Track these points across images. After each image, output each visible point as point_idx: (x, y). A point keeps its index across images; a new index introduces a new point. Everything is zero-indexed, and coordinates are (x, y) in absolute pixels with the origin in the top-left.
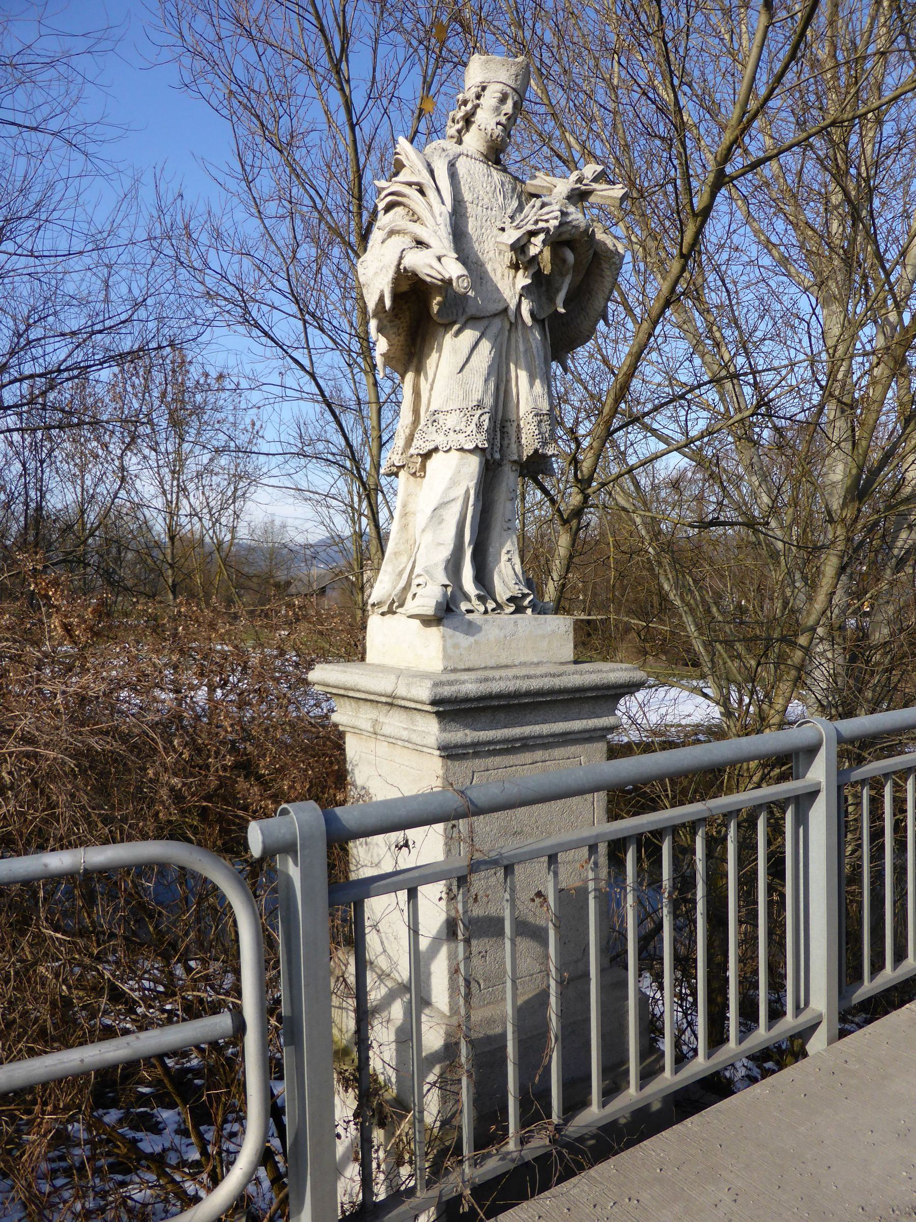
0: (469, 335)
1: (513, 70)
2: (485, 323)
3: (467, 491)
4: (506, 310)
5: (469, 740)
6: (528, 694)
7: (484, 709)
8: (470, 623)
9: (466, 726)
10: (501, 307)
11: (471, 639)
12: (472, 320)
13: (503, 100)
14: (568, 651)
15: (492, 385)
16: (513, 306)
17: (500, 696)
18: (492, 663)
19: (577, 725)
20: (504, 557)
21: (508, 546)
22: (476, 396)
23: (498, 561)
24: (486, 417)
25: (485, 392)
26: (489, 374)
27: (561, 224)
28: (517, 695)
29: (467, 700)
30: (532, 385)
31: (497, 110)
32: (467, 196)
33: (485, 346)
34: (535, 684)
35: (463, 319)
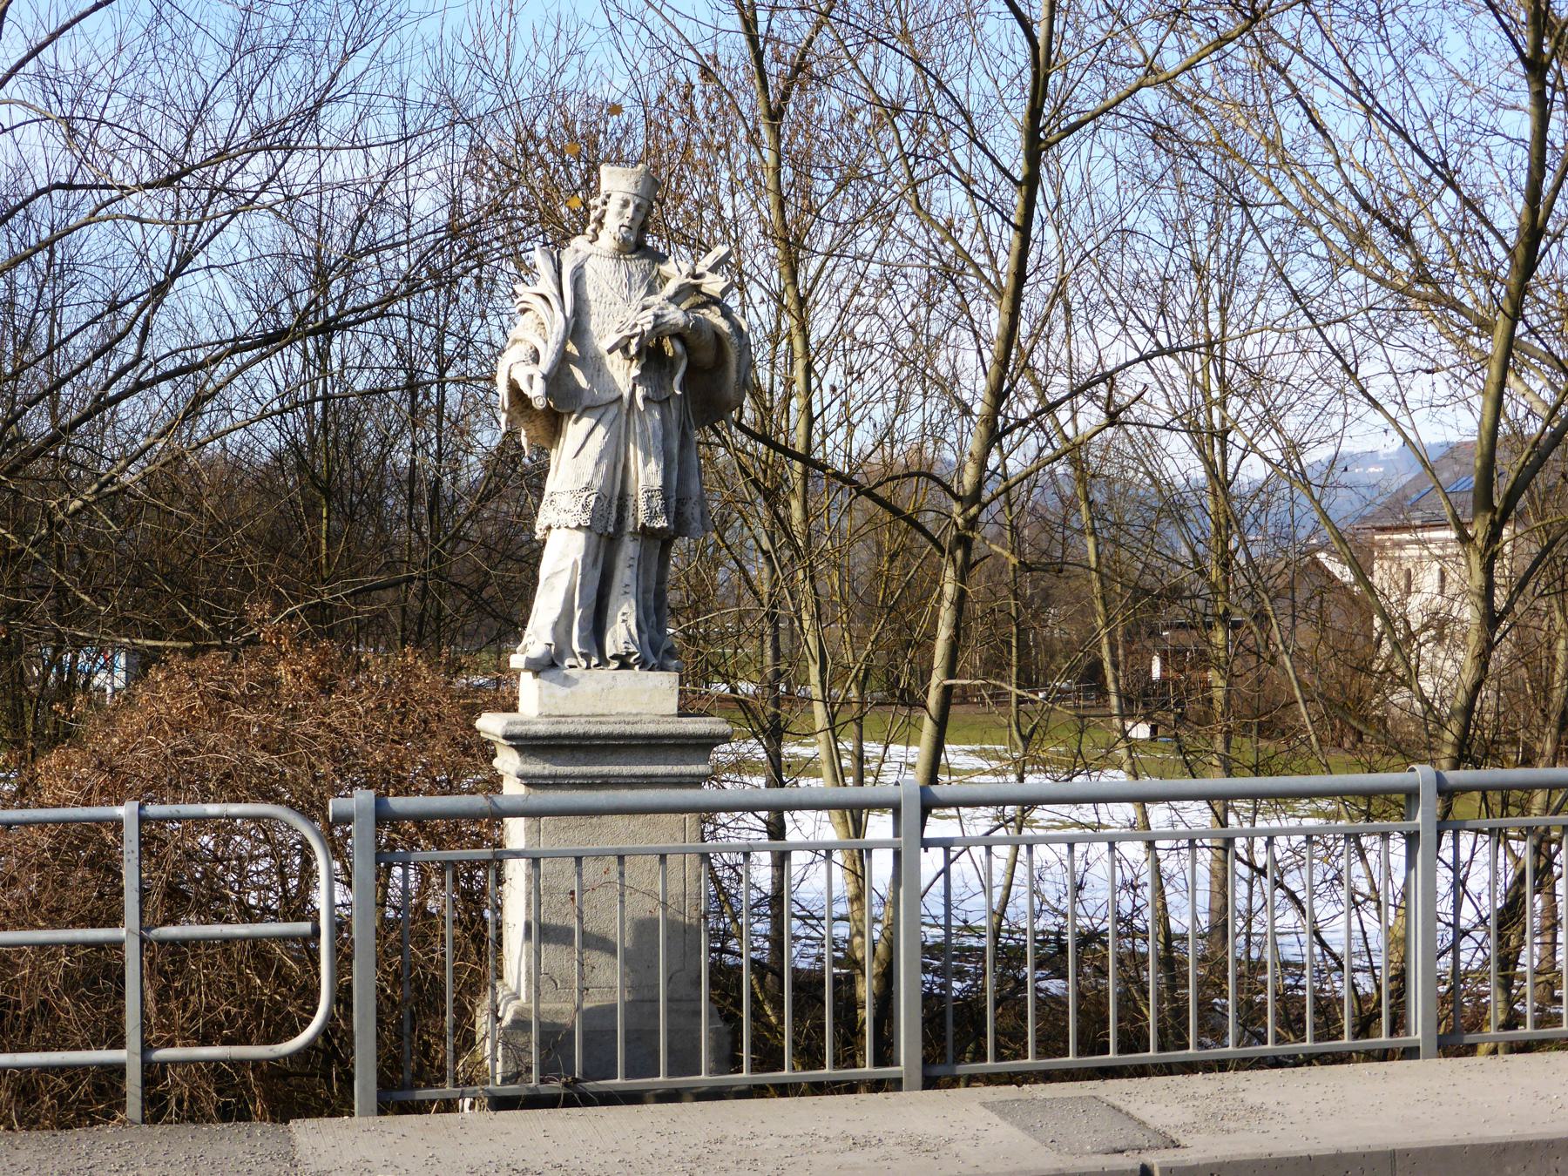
0: (587, 423)
1: (633, 179)
2: (598, 413)
3: (575, 562)
4: (621, 397)
5: (546, 772)
6: (598, 736)
7: (562, 747)
8: (566, 677)
9: (546, 761)
10: (616, 395)
11: (567, 690)
12: (586, 410)
13: (625, 204)
14: (672, 705)
15: (603, 468)
16: (626, 395)
17: (569, 736)
18: (588, 712)
20: (620, 618)
21: (625, 608)
22: (587, 479)
23: (614, 622)
24: (593, 498)
25: (595, 474)
26: (601, 458)
27: (654, 328)
28: (586, 736)
29: (536, 737)
30: (645, 465)
31: (620, 215)
32: (591, 294)
33: (601, 430)
34: (604, 729)
35: (579, 410)
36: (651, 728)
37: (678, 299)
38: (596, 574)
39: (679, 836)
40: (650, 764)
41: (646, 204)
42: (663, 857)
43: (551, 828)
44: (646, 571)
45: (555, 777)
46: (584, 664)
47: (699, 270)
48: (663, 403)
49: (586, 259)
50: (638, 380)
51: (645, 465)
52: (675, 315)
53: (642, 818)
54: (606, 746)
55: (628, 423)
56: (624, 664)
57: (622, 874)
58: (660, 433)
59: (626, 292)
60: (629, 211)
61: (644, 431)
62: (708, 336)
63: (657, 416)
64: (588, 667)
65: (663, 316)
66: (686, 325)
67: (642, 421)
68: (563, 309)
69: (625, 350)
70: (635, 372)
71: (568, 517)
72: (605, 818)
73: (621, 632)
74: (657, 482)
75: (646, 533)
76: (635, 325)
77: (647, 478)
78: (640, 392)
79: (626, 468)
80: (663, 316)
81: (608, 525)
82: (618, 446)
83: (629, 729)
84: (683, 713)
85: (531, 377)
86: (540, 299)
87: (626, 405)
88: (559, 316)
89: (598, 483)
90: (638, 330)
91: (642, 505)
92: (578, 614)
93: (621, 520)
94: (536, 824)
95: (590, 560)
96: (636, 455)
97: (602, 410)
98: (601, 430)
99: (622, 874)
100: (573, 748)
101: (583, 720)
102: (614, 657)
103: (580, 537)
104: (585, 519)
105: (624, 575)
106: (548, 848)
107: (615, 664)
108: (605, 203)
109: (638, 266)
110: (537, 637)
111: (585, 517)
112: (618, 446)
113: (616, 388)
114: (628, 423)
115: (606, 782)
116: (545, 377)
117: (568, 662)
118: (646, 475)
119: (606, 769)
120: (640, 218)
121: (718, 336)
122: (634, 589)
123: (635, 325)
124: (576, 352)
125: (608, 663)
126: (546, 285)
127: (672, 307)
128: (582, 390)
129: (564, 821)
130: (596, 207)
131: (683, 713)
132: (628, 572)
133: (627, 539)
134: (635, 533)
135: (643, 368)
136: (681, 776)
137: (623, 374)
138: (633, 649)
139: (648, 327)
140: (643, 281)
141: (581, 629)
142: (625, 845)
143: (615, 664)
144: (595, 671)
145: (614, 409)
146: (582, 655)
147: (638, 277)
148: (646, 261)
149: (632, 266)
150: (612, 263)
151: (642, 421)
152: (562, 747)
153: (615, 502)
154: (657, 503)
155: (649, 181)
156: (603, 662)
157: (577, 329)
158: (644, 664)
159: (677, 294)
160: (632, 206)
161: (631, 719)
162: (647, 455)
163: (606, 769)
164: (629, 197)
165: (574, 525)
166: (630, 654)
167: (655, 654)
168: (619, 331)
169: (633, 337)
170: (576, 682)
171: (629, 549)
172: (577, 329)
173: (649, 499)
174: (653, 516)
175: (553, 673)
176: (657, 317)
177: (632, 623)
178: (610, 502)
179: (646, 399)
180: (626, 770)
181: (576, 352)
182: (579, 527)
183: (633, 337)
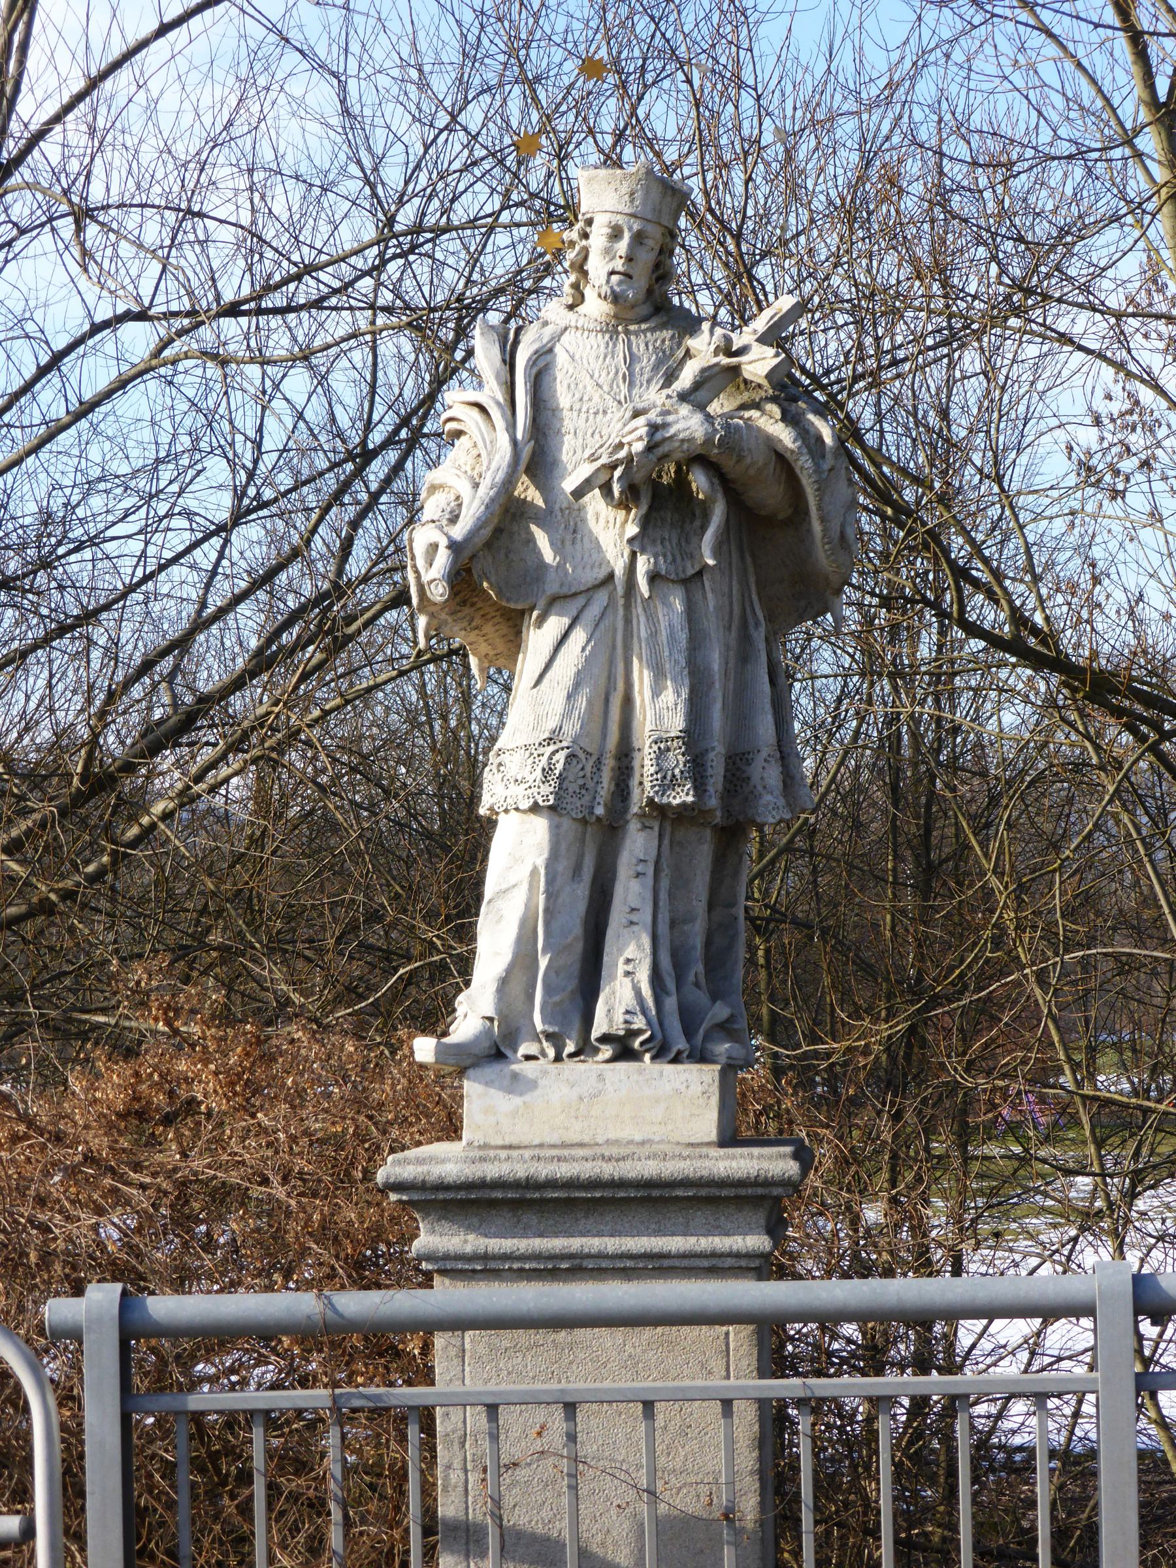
0: (555, 624)
1: (625, 189)
2: (574, 606)
3: (534, 872)
4: (611, 576)
5: (468, 1249)
6: (552, 1184)
7: (493, 1204)
8: (515, 1076)
9: (470, 1228)
10: (602, 574)
11: (517, 1101)
12: (555, 602)
13: (616, 234)
14: (707, 1125)
15: (582, 703)
16: (619, 569)
17: (499, 1184)
18: (554, 1139)
19: (704, 1243)
20: (621, 968)
21: (630, 951)
22: (552, 724)
23: (613, 977)
24: (561, 757)
25: (567, 714)
26: (577, 685)
27: (650, 448)
28: (530, 1184)
29: (441, 1186)
30: (656, 693)
31: (608, 252)
32: (563, 397)
33: (579, 636)
34: (565, 1171)
35: (542, 603)
36: (648, 1169)
37: (701, 395)
38: (578, 896)
39: (717, 1365)
40: (658, 1233)
41: (655, 232)
42: (648, 1406)
43: (482, 1349)
44: (680, 883)
45: (485, 1257)
46: (551, 1053)
47: (738, 342)
48: (691, 582)
49: (557, 337)
50: (637, 544)
51: (656, 693)
52: (688, 424)
53: (648, 1333)
54: (570, 1203)
55: (628, 621)
56: (624, 1049)
57: (572, 1437)
58: (683, 636)
59: (624, 389)
60: (622, 246)
61: (654, 635)
62: (759, 457)
63: (678, 605)
64: (558, 1058)
65: (665, 425)
66: (708, 441)
67: (651, 618)
68: (511, 426)
69: (606, 489)
70: (632, 530)
71: (520, 790)
72: (581, 1333)
73: (625, 991)
74: (676, 723)
75: (658, 811)
76: (620, 445)
77: (659, 718)
78: (643, 565)
79: (628, 701)
80: (665, 425)
81: (592, 803)
82: (611, 662)
83: (607, 1170)
84: (729, 1138)
85: (434, 547)
86: (475, 413)
87: (620, 590)
88: (503, 440)
89: (571, 729)
90: (622, 454)
91: (649, 768)
92: (543, 962)
93: (622, 791)
94: (456, 1341)
95: (563, 866)
96: (642, 679)
97: (581, 601)
98: (579, 636)
99: (572, 1437)
100: (517, 1205)
101: (527, 1154)
102: (605, 1039)
103: (540, 826)
104: (546, 793)
105: (630, 891)
106: (480, 1387)
107: (607, 1051)
108: (585, 236)
109: (648, 343)
110: (473, 1011)
111: (546, 789)
112: (611, 662)
113: (604, 562)
114: (628, 621)
115: (578, 1267)
116: (453, 546)
117: (524, 1049)
118: (660, 711)
119: (575, 1244)
120: (646, 257)
121: (780, 458)
122: (646, 916)
123: (620, 445)
124: (540, 502)
125: (596, 1051)
126: (491, 393)
127: (685, 410)
128: (542, 566)
129: (505, 1338)
130: (572, 244)
131: (729, 1138)
132: (635, 886)
133: (634, 826)
134: (642, 816)
135: (646, 523)
136: (714, 1255)
137: (611, 530)
138: (639, 1023)
139: (638, 447)
140: (655, 368)
141: (548, 990)
142: (576, 1384)
143: (607, 1051)
144: (571, 1068)
145: (601, 598)
146: (549, 1036)
147: (646, 362)
148: (667, 334)
149: (639, 345)
150: (601, 340)
151: (651, 618)
152: (493, 1204)
153: (609, 763)
154: (677, 760)
155: (656, 191)
156: (585, 1049)
157: (537, 456)
158: (662, 1051)
159: (697, 385)
160: (627, 236)
161: (615, 1151)
162: (659, 675)
163: (575, 1244)
164: (621, 220)
165: (525, 804)
166: (632, 1034)
167: (689, 1033)
168: (593, 458)
169: (613, 467)
170: (533, 1085)
171: (638, 844)
172: (537, 456)
173: (661, 754)
174: (668, 783)
175: (491, 1071)
176: (654, 428)
177: (643, 976)
178: (599, 762)
179: (654, 578)
180: (611, 1244)
181: (540, 502)
182: (535, 808)
183: (613, 467)
